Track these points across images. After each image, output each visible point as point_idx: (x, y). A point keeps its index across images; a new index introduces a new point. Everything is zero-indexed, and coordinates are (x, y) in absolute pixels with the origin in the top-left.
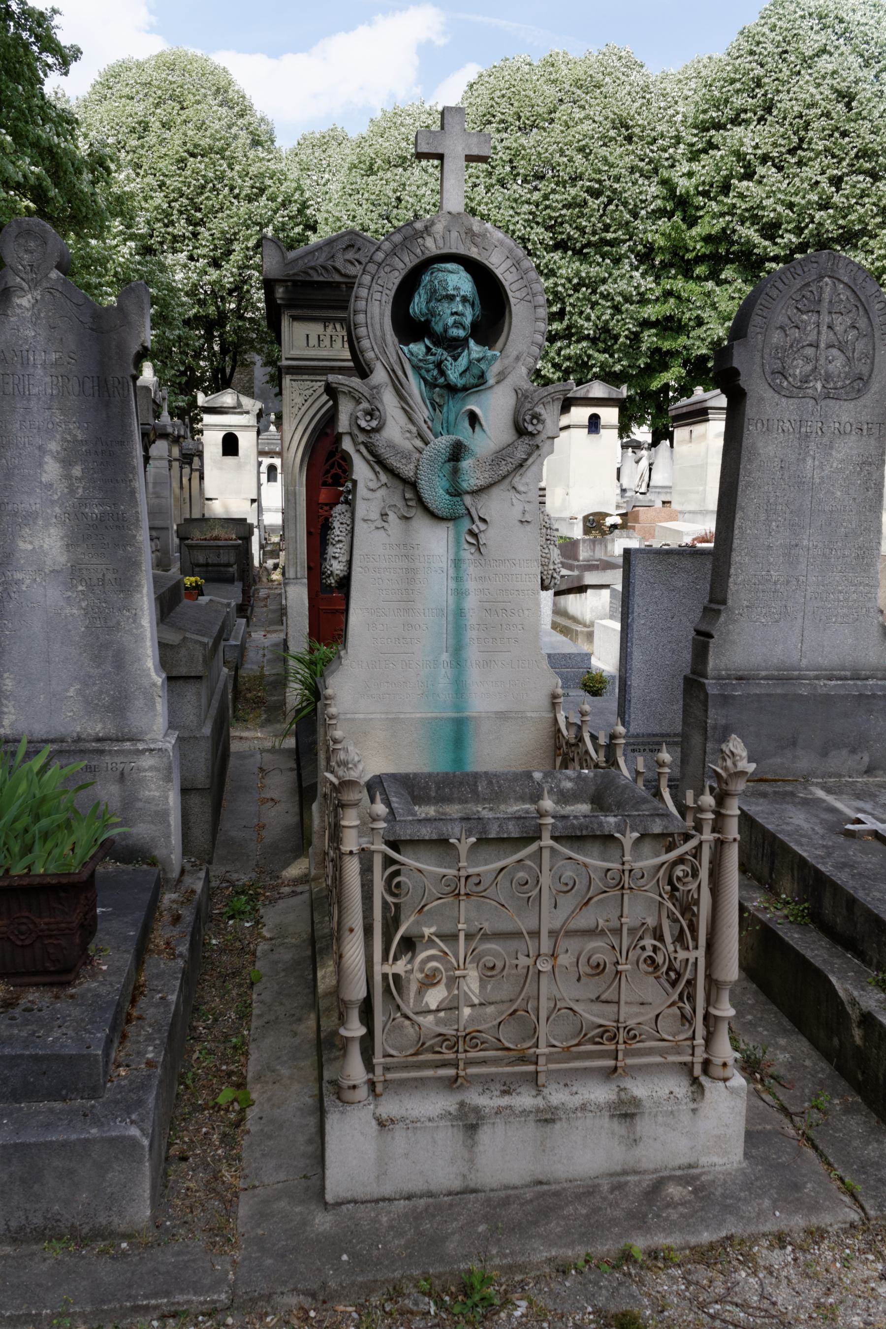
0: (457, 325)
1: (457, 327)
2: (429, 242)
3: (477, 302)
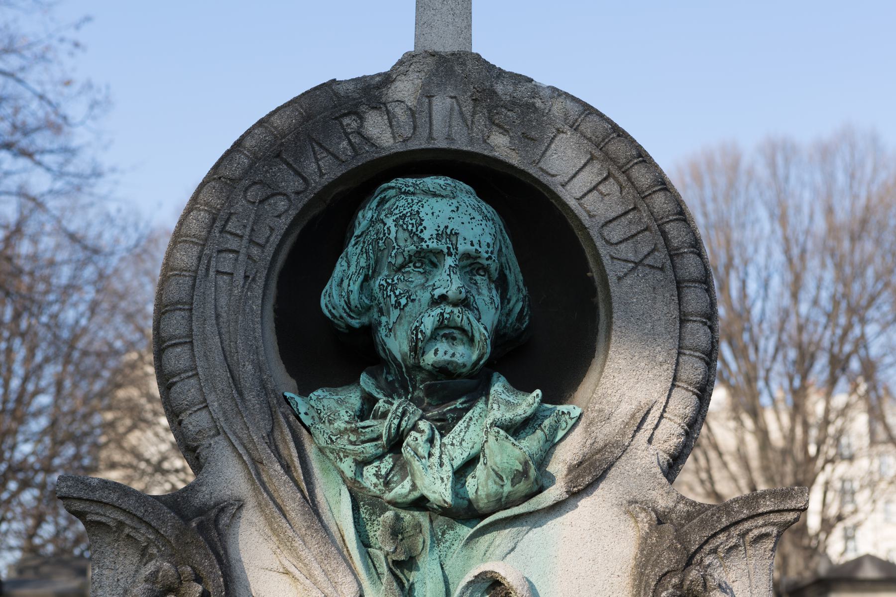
0: (446, 330)
1: (451, 338)
3: (515, 275)
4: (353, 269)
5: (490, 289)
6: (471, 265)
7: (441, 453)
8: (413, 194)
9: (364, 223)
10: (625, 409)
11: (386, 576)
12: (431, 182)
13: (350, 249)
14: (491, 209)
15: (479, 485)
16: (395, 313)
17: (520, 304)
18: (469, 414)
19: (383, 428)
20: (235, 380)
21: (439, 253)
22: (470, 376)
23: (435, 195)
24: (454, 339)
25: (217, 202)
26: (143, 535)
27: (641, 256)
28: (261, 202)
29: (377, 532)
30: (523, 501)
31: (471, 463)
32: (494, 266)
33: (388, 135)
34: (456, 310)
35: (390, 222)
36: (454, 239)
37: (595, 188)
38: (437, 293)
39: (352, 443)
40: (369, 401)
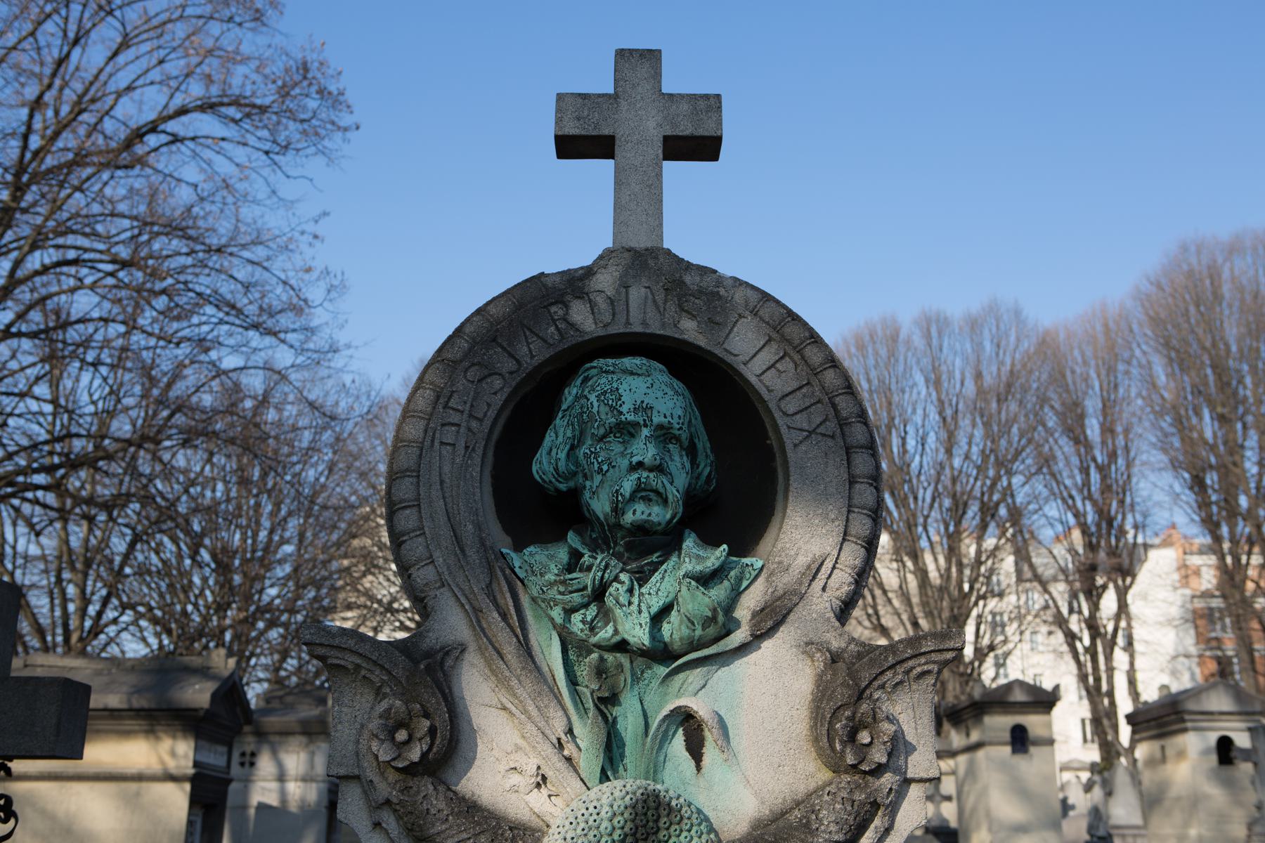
0: (642, 493)
1: (647, 500)
2: (580, 314)
3: (703, 443)
4: (560, 439)
5: (681, 456)
6: (664, 435)
7: (640, 601)
8: (613, 373)
9: (570, 399)
10: (802, 561)
11: (592, 711)
12: (628, 362)
13: (558, 421)
14: (681, 385)
15: (673, 630)
16: (598, 478)
17: (708, 469)
18: (664, 567)
19: (588, 579)
20: (457, 538)
21: (636, 425)
22: (665, 533)
23: (632, 373)
24: (650, 500)
25: (440, 382)
26: (377, 676)
27: (814, 426)
28: (479, 381)
29: (584, 671)
30: (713, 644)
31: (666, 610)
32: (684, 436)
33: (591, 321)
34: (651, 475)
35: (593, 398)
36: (649, 412)
37: (773, 366)
38: (635, 460)
39: (561, 593)
40: (576, 555)
